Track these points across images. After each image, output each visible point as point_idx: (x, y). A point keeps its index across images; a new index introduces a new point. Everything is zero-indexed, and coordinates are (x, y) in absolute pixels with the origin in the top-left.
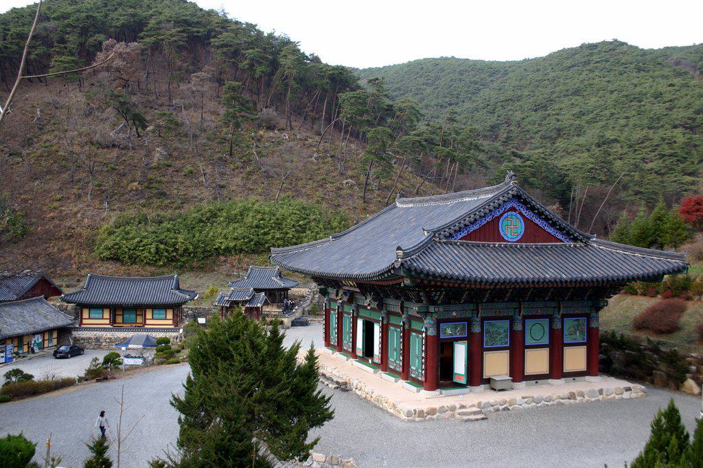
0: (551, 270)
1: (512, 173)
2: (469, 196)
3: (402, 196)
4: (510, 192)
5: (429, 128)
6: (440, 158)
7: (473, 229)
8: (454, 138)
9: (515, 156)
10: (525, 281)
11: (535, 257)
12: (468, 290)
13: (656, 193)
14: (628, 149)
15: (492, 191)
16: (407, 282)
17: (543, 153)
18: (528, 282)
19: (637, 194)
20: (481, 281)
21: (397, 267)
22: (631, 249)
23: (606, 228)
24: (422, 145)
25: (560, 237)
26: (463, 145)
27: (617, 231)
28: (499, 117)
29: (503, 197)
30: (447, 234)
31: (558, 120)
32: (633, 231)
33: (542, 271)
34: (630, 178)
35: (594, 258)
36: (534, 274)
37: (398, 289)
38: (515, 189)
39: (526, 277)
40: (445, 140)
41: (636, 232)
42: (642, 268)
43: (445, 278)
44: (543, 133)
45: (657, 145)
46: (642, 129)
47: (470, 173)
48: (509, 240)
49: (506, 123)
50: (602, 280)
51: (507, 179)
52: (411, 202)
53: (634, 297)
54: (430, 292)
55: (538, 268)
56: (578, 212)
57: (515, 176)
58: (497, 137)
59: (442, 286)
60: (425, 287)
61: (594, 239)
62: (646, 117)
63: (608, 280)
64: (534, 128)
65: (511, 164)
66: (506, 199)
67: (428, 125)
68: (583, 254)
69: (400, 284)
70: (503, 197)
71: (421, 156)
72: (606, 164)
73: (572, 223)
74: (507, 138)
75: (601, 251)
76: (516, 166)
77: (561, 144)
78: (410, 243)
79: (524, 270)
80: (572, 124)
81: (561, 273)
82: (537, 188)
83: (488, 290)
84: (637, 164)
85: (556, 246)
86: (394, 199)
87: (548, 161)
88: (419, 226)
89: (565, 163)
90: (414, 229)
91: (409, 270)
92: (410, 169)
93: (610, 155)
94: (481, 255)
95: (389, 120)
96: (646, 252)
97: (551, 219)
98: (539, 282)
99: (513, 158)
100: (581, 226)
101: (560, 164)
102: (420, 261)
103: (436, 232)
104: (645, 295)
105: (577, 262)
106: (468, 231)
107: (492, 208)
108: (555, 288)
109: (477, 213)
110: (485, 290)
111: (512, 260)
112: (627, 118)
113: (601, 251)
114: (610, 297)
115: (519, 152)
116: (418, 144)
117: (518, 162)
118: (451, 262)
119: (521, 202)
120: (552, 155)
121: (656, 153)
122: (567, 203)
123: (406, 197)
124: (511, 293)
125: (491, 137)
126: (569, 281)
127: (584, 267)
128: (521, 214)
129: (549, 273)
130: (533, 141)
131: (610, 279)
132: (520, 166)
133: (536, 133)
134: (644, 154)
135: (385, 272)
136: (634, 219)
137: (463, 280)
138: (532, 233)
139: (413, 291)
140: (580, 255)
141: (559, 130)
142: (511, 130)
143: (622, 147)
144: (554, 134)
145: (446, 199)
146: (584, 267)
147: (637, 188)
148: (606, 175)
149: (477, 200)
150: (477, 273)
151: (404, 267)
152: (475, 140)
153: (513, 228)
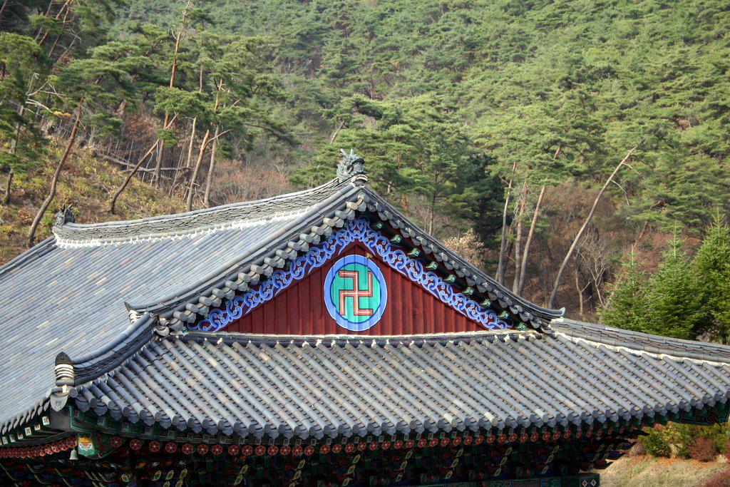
0: (457, 402)
1: (353, 156)
2: (246, 214)
3: (69, 218)
4: (349, 204)
5: (142, 39)
6: (170, 118)
7: (258, 301)
8: (207, 65)
9: (364, 112)
10: (392, 432)
11: (415, 369)
12: (248, 461)
13: (707, 203)
14: (637, 94)
15: (305, 203)
16: (86, 447)
17: (432, 104)
18: (399, 435)
19: (661, 205)
20: (282, 437)
21: (57, 408)
22: (650, 343)
23: (590, 291)
24: (124, 85)
25: (477, 316)
26: (230, 84)
27: (616, 299)
28: (321, 10)
29: (332, 217)
30: (191, 317)
31: (469, 21)
32: (655, 296)
33: (433, 406)
34: (644, 166)
35: (562, 368)
36: (414, 412)
37: (61, 467)
38: (361, 196)
39: (395, 422)
40: (182, 71)
41: (662, 299)
42: (678, 390)
43: (187, 431)
44: (431, 52)
45: (708, 84)
46: (672, 44)
47: (248, 156)
48: (355, 328)
49: (339, 26)
50: (596, 421)
51: (342, 173)
52: (95, 234)
53: (662, 461)
54: (149, 471)
55: (422, 397)
56: (521, 253)
57: (362, 162)
58: (316, 62)
59: (179, 455)
60: (135, 457)
61: (561, 320)
62: (679, 11)
63: (596, 422)
64: (409, 40)
65: (352, 133)
66: (340, 224)
67: (139, 30)
68: (534, 358)
69: (68, 453)
70: (332, 217)
71: (121, 111)
72: (588, 136)
73: (508, 281)
74: (344, 66)
75: (578, 350)
76: (364, 137)
77: (474, 81)
78: (92, 341)
79: (389, 404)
80: (504, 31)
81: (481, 409)
82: (420, 192)
83: (298, 459)
84: (661, 129)
85: (468, 341)
86: (50, 225)
87: (444, 125)
88: (117, 296)
89: (487, 129)
90: (105, 303)
91: (91, 415)
92: (91, 147)
93: (594, 108)
94: (278, 369)
95: (34, 17)
96: (685, 348)
97: (453, 272)
98: (427, 432)
99: (358, 117)
100: (527, 289)
101: (474, 131)
102: (121, 389)
103: (158, 313)
104: (688, 457)
105: (520, 378)
106: (246, 308)
107: (305, 247)
108: (467, 448)
109: (267, 260)
110: (293, 461)
111: (358, 378)
112: (635, 15)
113: (578, 350)
114: (605, 466)
115: (373, 103)
116: (111, 80)
117: (371, 126)
118: (199, 390)
119: (377, 230)
120: (455, 109)
121: (706, 103)
122: (494, 231)
123: (83, 222)
124: (360, 464)
125: (301, 62)
126: (502, 427)
127: (537, 390)
128: (377, 259)
129: (451, 408)
130: (406, 73)
131: (603, 419)
132: (375, 137)
133: (415, 53)
134: (677, 107)
135: (25, 425)
136: (656, 266)
137: (235, 435)
138: (407, 311)
139: (104, 471)
140: (526, 362)
141: (471, 45)
142: (353, 47)
143: (624, 88)
144: (458, 56)
145: (187, 225)
146: (537, 390)
147: (662, 189)
148: (586, 159)
149: (268, 226)
150: (269, 416)
151: (76, 408)
152: (260, 71)
153: (358, 298)
